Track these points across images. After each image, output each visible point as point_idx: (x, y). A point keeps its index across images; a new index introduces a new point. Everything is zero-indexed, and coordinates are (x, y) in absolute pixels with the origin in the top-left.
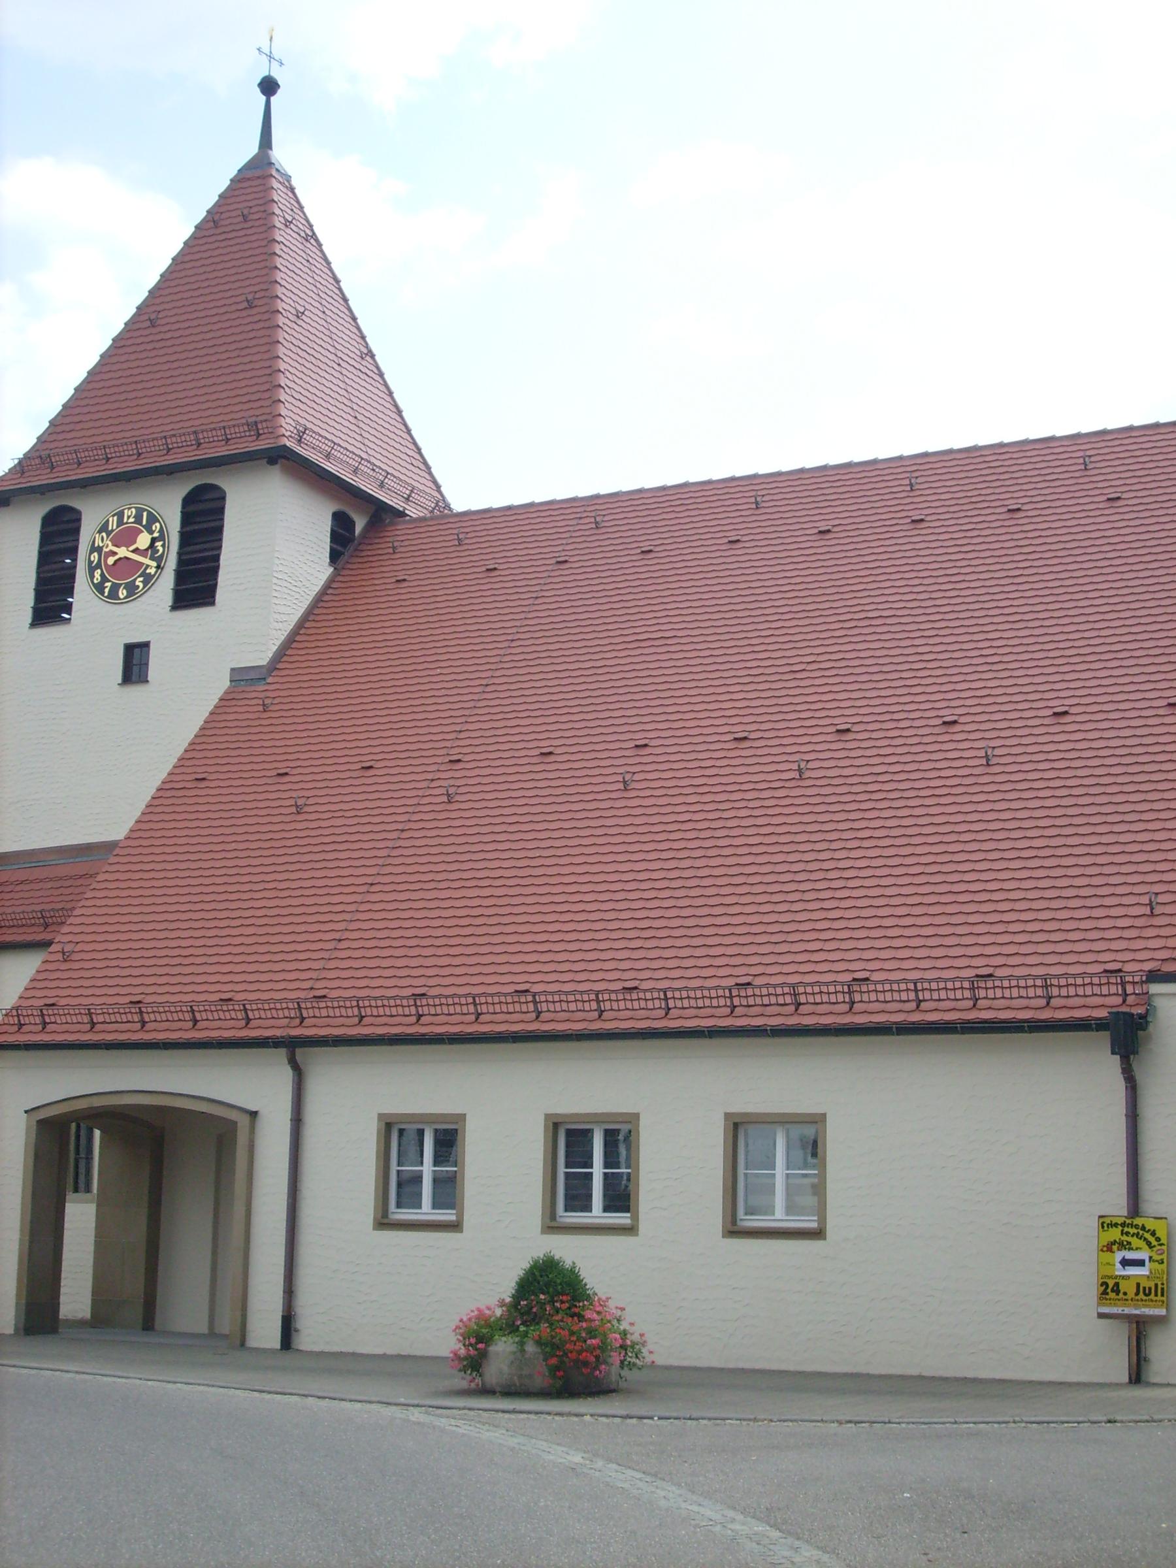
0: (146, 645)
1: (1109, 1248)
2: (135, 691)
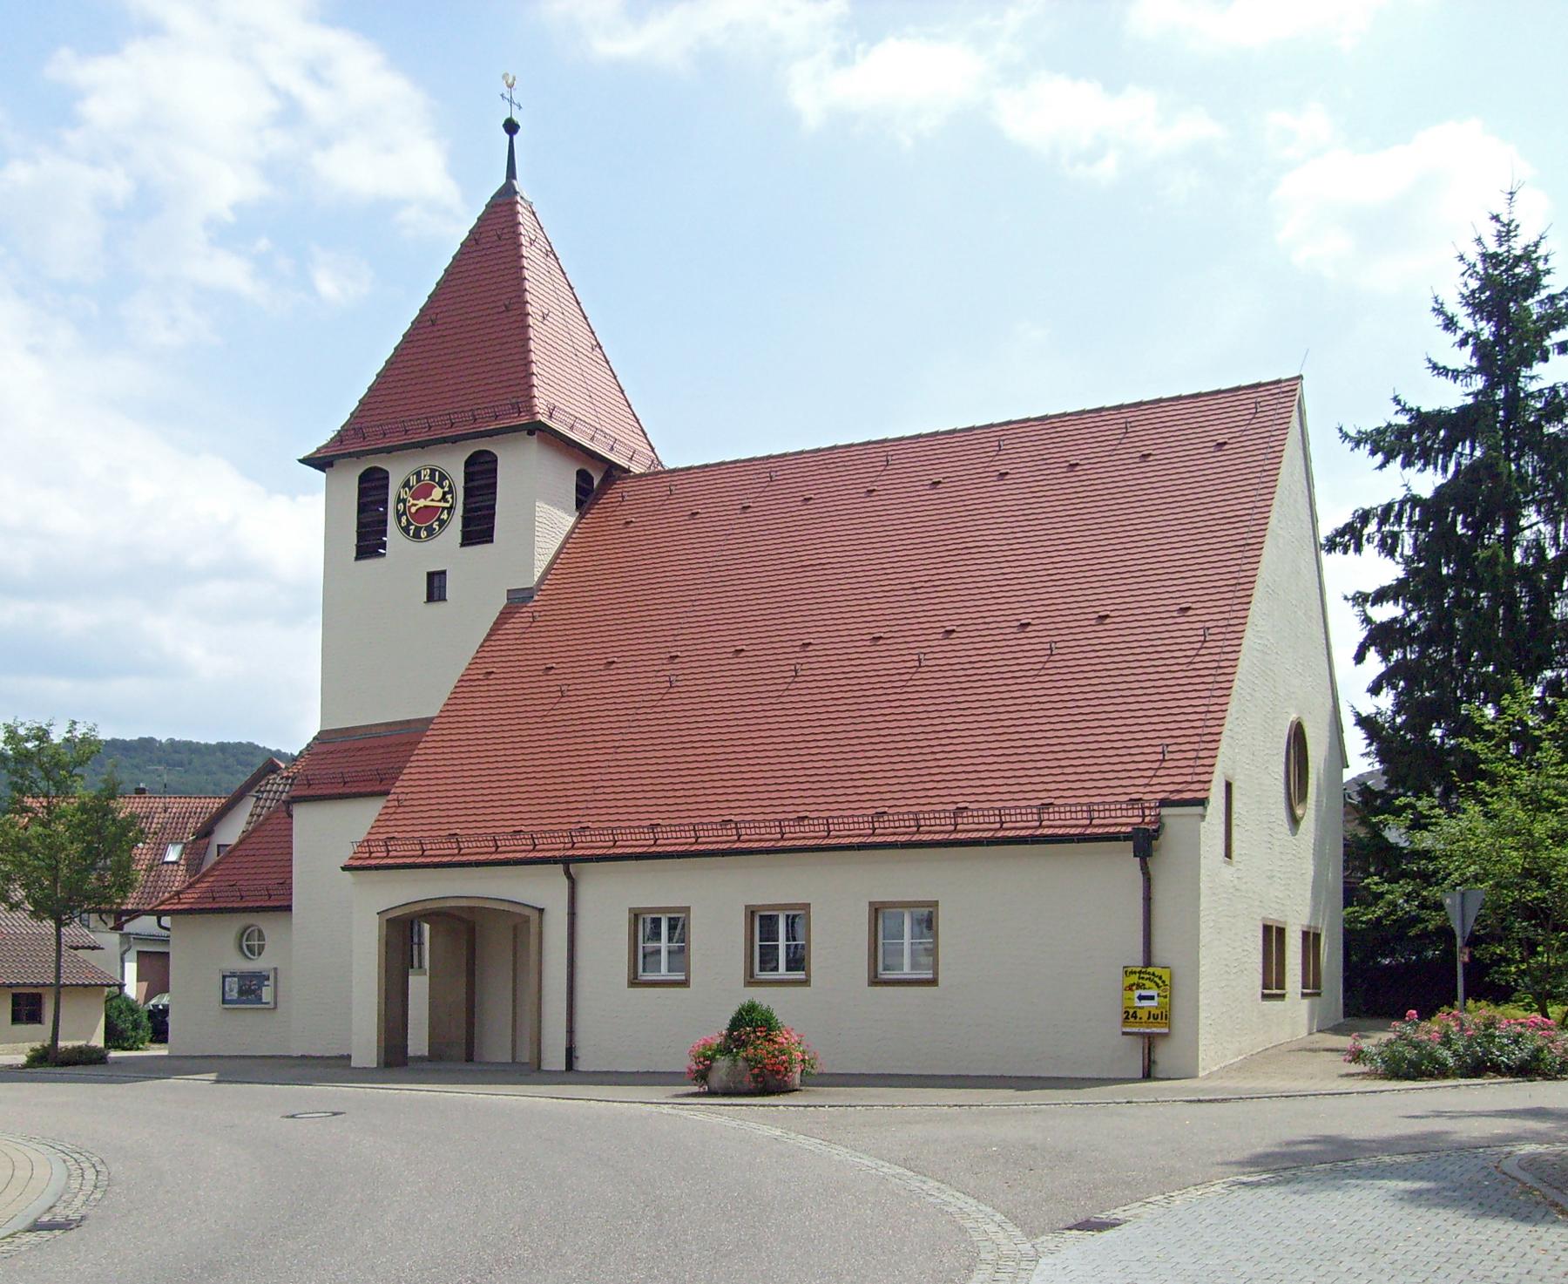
0: (444, 572)
1: (1130, 988)
2: (436, 607)
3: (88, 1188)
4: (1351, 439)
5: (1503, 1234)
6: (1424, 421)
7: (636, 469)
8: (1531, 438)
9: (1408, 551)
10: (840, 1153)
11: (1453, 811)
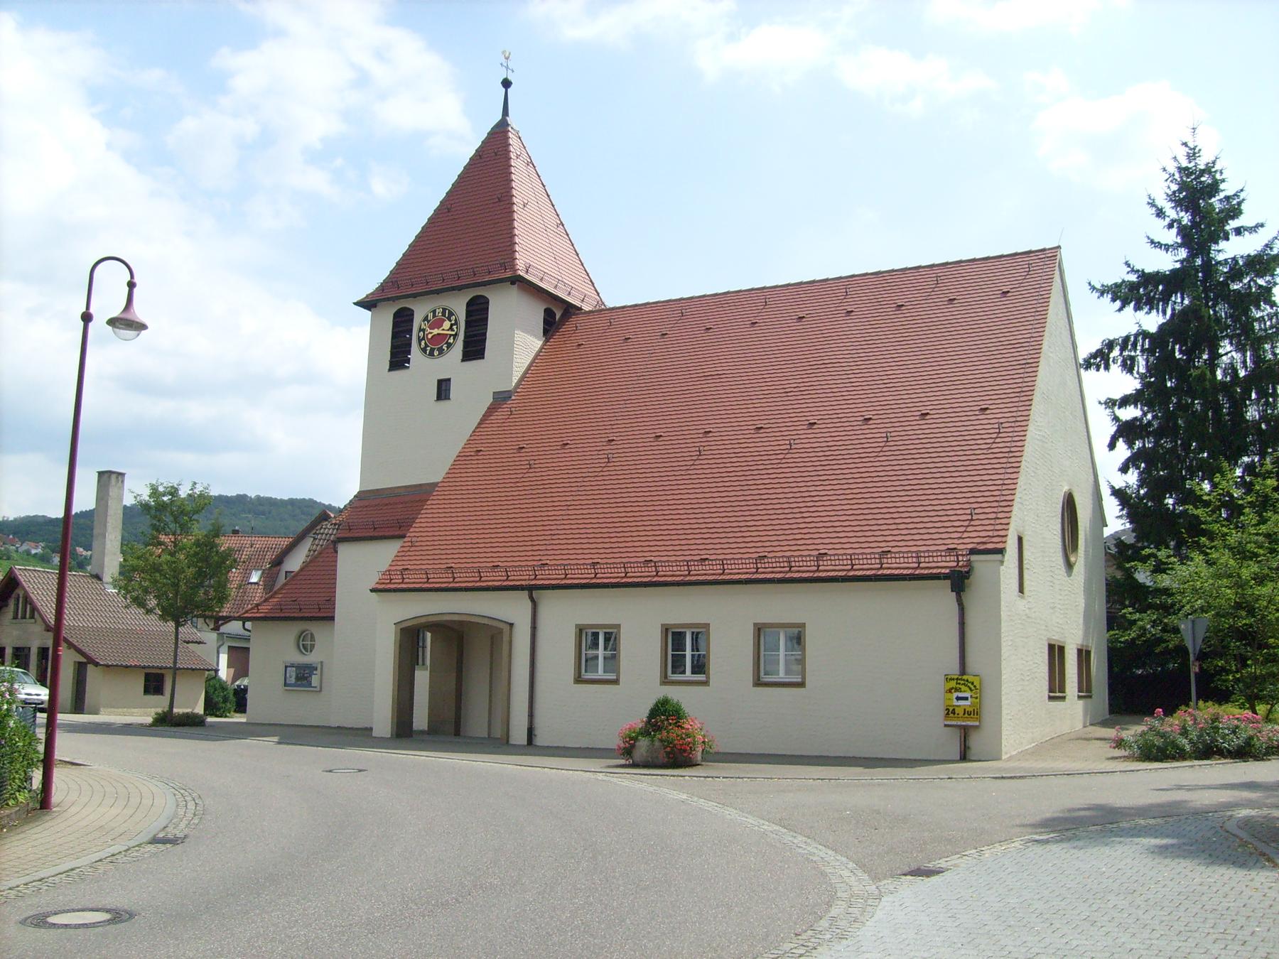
1: (950, 691)
2: (443, 404)
3: (190, 815)
4: (1098, 290)
5: (1226, 877)
6: (1148, 279)
7: (586, 308)
8: (1222, 292)
9: (1142, 370)
10: (731, 813)
11: (1184, 559)
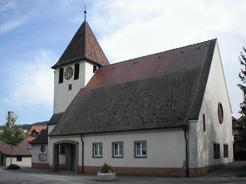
0: (71, 85)
